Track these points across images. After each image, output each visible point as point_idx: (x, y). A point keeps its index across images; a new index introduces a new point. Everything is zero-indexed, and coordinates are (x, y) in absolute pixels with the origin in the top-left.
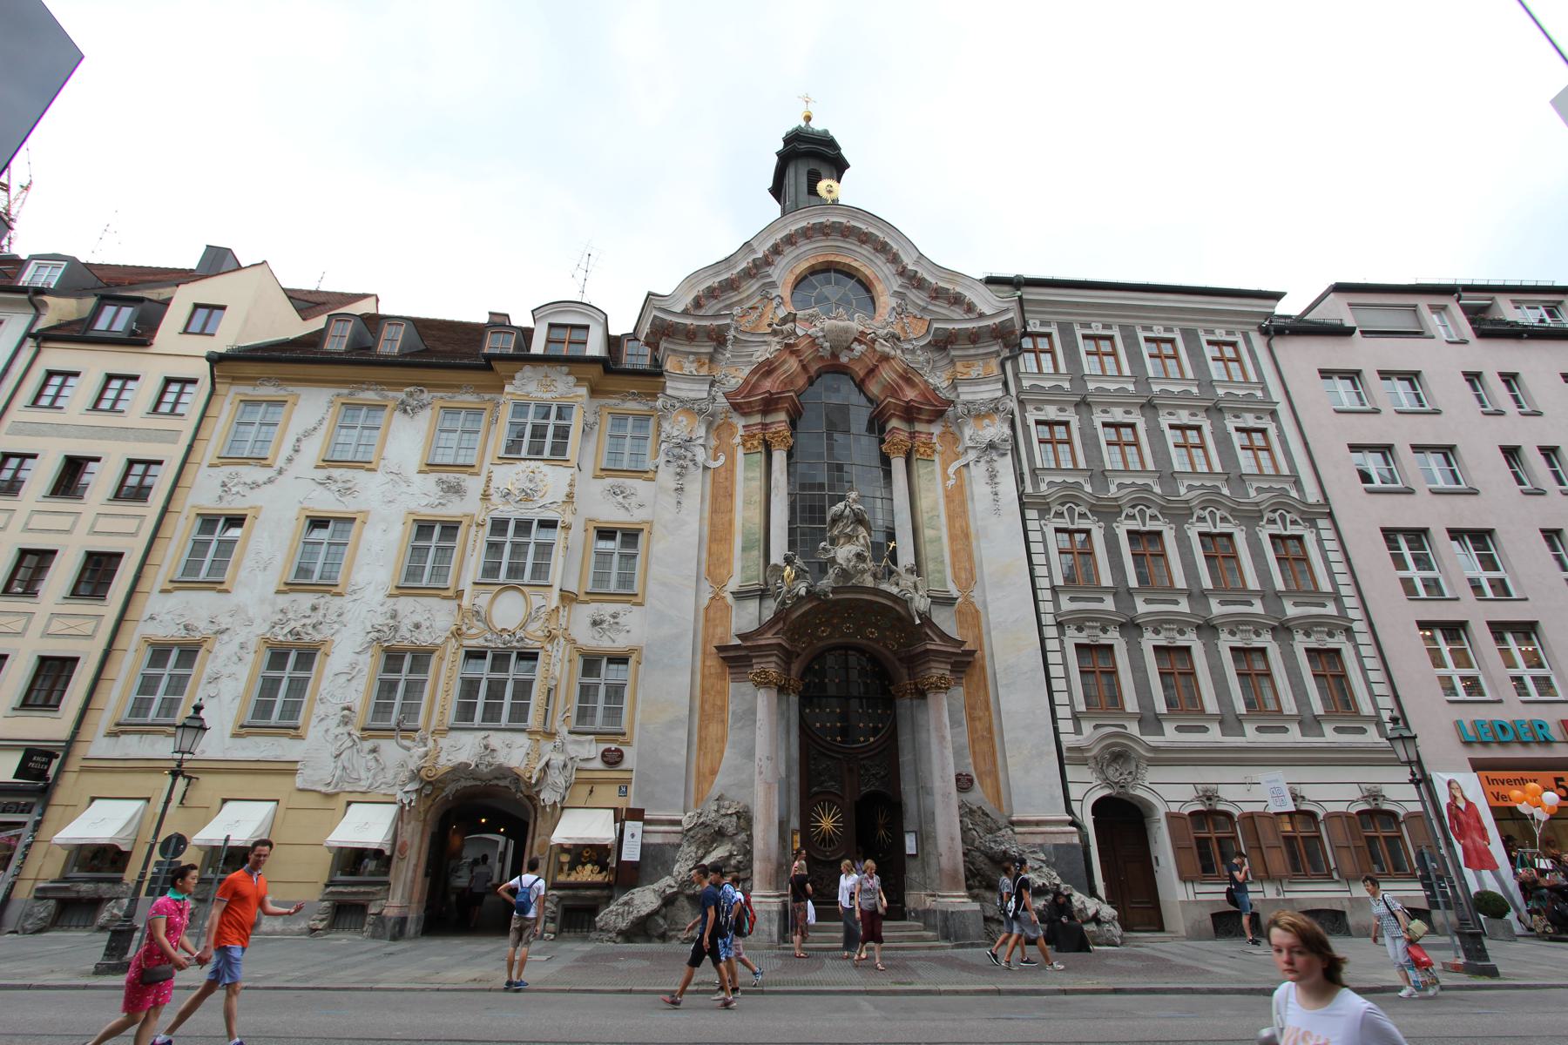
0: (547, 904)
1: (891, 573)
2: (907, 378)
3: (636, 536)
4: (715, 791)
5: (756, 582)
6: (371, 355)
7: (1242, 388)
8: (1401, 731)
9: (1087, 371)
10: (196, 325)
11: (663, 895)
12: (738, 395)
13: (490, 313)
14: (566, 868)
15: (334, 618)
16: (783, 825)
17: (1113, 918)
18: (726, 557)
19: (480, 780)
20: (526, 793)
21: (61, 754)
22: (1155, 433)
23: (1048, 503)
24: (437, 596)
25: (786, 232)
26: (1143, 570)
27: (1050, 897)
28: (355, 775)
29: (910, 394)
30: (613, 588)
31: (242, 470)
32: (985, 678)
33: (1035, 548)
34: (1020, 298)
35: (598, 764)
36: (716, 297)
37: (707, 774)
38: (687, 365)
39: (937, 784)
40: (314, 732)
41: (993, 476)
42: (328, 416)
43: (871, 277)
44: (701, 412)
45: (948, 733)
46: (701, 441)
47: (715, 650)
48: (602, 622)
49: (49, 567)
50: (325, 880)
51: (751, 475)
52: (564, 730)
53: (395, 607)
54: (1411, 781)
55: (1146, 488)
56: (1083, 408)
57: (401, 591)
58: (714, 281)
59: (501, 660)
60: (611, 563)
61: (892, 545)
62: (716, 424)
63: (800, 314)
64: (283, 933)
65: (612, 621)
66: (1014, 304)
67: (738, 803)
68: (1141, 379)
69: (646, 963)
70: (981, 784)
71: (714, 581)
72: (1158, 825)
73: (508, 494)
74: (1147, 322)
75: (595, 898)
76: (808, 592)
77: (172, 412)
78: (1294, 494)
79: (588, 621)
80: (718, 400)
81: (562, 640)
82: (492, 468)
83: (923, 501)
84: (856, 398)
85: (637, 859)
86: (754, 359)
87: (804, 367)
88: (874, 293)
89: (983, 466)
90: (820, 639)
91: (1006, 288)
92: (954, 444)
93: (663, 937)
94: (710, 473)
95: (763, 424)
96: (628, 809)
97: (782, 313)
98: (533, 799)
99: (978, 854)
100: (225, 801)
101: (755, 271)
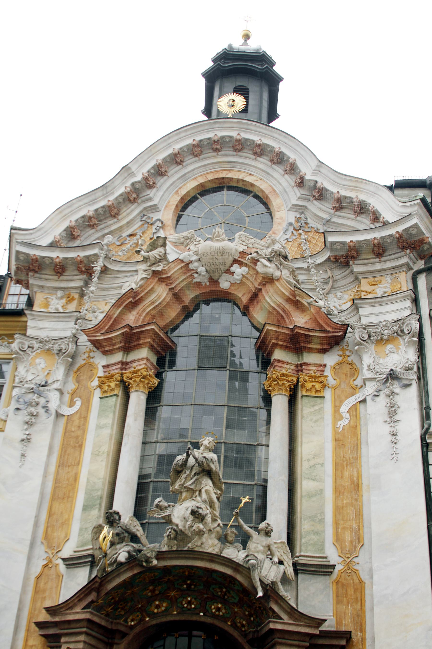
12: (97, 332)
18: (66, 516)
25: (170, 151)
36: (92, 226)
43: (267, 192)
51: (104, 421)
62: (77, 366)
66: (416, 208)
71: (50, 546)
83: (304, 446)
88: (271, 209)
89: (382, 400)
90: (153, 615)
92: (352, 375)
94: (63, 422)
95: (122, 363)
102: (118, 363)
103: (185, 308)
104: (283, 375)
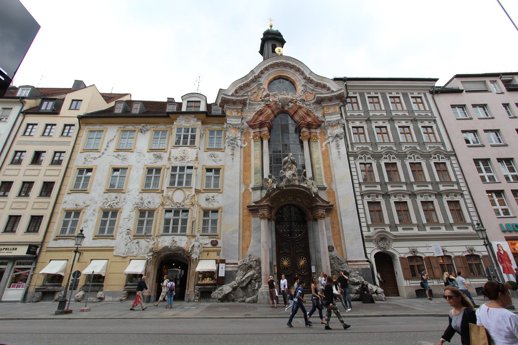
0: (195, 291)
1: (304, 180)
2: (308, 114)
3: (219, 170)
4: (248, 253)
5: (260, 184)
6: (130, 114)
7: (423, 113)
8: (480, 228)
9: (369, 109)
10: (73, 107)
11: (233, 287)
13: (168, 98)
14: (201, 279)
15: (123, 201)
16: (271, 264)
17: (382, 292)
18: (249, 176)
19: (172, 251)
20: (187, 255)
21: (40, 246)
22: (394, 129)
23: (357, 155)
24: (155, 192)
25: (265, 66)
26: (390, 176)
27: (361, 285)
28: (132, 251)
29: (309, 119)
30: (212, 188)
31: (91, 153)
32: (337, 214)
33: (353, 170)
34: (346, 85)
35: (210, 245)
36: (242, 89)
37: (245, 248)
38: (234, 113)
39: (322, 249)
40: (118, 237)
41: (338, 146)
42: (117, 135)
44: (239, 128)
45: (325, 232)
46: (239, 138)
47: (246, 207)
48: (209, 199)
49: (32, 187)
50: (124, 284)
51: (256, 149)
52: (198, 235)
53: (142, 196)
54: (484, 245)
55: (391, 148)
56: (368, 122)
57: (144, 191)
58: (241, 84)
59: (177, 213)
60: (211, 180)
61: (304, 170)
62: (244, 132)
63: (271, 94)
64: (112, 301)
65: (212, 199)
66: (344, 87)
67: (256, 257)
68: (388, 111)
69: (228, 309)
70: (337, 249)
72: (397, 261)
73: (177, 158)
74: (390, 91)
75: (211, 288)
76: (277, 187)
77: (67, 136)
78: (442, 148)
79: (205, 199)
80: (244, 124)
81: (196, 205)
82: (171, 150)
83: (314, 155)
84: (290, 121)
85: (224, 275)
86: (256, 110)
87: (273, 112)
89: (334, 143)
90: (281, 202)
91: (341, 82)
92: (325, 136)
93: (233, 300)
94: (242, 149)
95: (260, 132)
96: (220, 260)
97: (265, 94)
98: (189, 257)
99: (336, 272)
100: (92, 260)
101: (255, 80)
102: (258, 132)
103: (275, 115)
104: (306, 135)
